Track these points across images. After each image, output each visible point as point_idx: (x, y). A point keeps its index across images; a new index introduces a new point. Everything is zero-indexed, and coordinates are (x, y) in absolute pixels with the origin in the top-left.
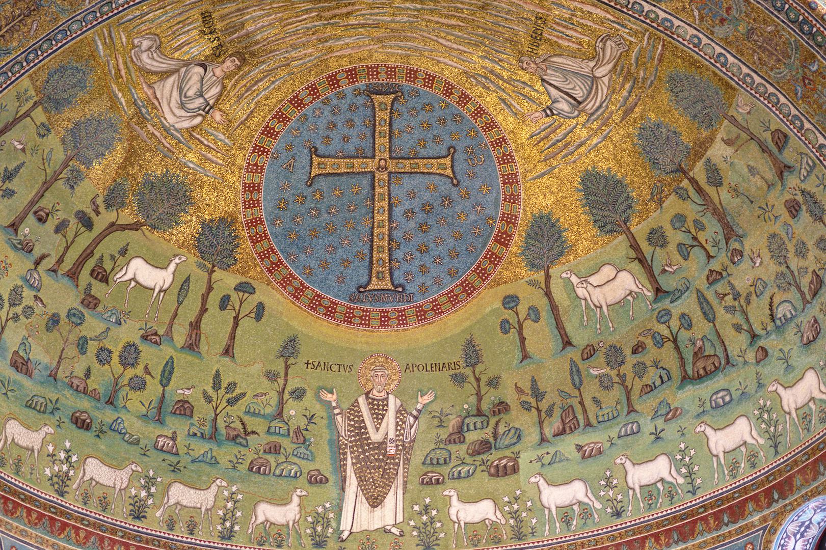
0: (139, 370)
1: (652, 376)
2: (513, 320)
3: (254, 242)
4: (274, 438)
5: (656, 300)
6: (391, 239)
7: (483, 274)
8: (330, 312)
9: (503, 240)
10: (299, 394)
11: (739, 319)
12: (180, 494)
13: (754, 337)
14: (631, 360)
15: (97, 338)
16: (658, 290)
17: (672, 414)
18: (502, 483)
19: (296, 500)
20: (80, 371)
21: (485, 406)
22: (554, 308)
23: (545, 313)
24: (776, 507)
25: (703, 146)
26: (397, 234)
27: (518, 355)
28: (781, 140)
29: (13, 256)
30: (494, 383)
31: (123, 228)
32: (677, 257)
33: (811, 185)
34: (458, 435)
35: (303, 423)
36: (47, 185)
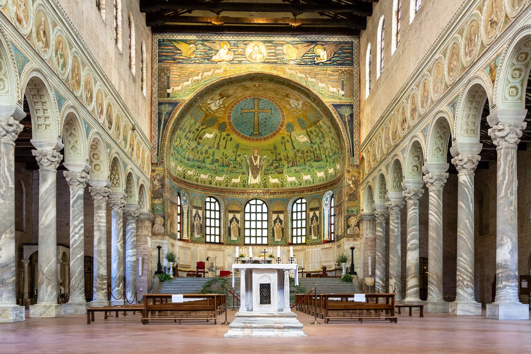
0: (208, 155)
1: (309, 158)
2: (283, 142)
3: (230, 126)
4: (235, 165)
5: (311, 144)
6: (258, 124)
7: (278, 132)
8: (246, 138)
9: (282, 126)
10: (239, 155)
11: (324, 152)
12: (218, 178)
13: (326, 157)
14: (306, 154)
15: (200, 150)
16: (311, 142)
17: (312, 167)
18: (280, 175)
19: (239, 178)
20: (198, 157)
21: (277, 159)
22: (292, 140)
23: (290, 142)
24: (325, 190)
25: (318, 121)
26: (260, 123)
27: (284, 149)
28: (330, 128)
29: (186, 141)
30: (279, 154)
31: (204, 129)
32: (315, 137)
33: (334, 136)
34: (272, 165)
35: (240, 161)
36: (191, 127)
